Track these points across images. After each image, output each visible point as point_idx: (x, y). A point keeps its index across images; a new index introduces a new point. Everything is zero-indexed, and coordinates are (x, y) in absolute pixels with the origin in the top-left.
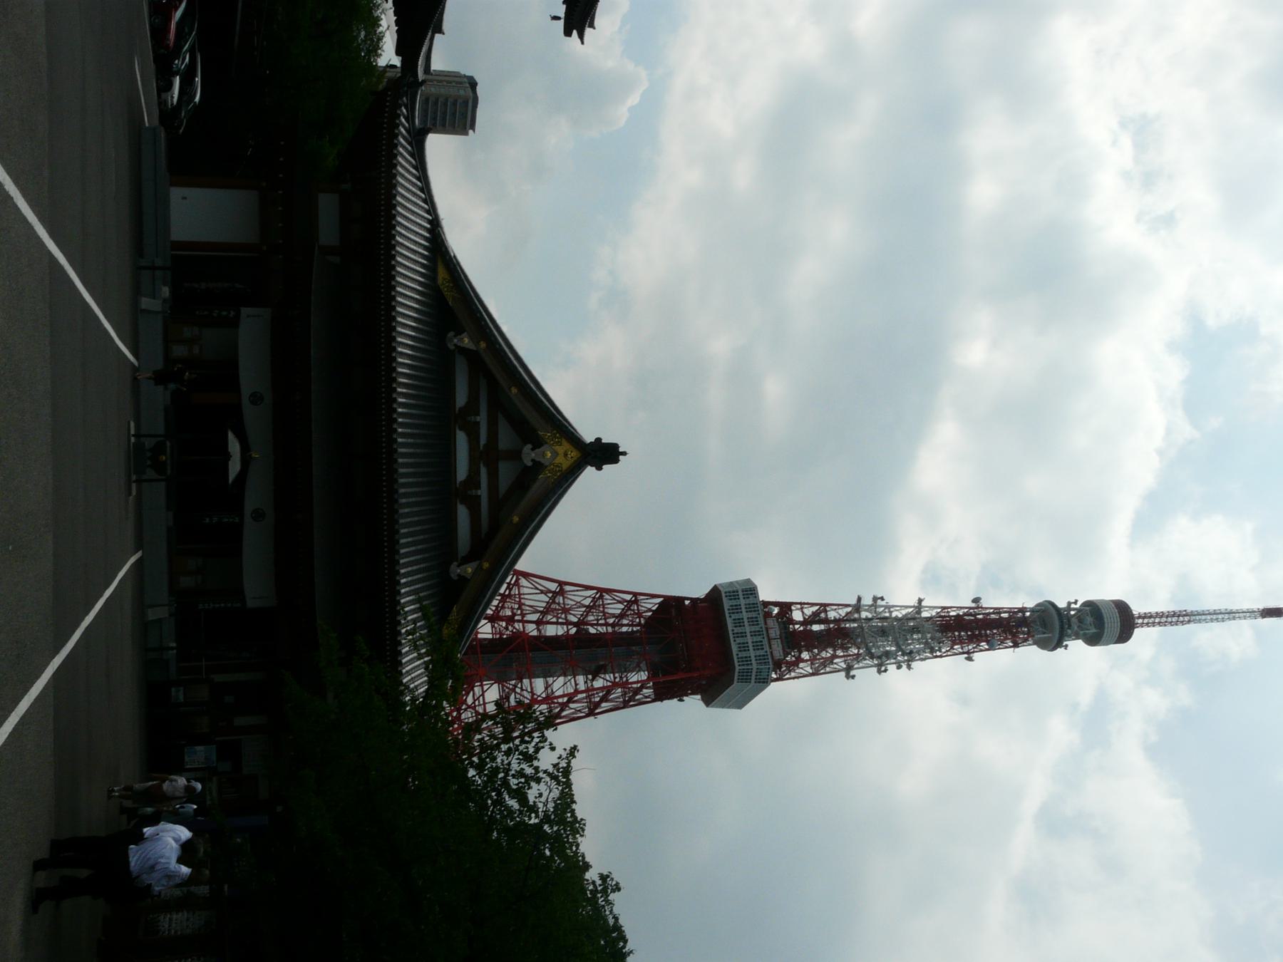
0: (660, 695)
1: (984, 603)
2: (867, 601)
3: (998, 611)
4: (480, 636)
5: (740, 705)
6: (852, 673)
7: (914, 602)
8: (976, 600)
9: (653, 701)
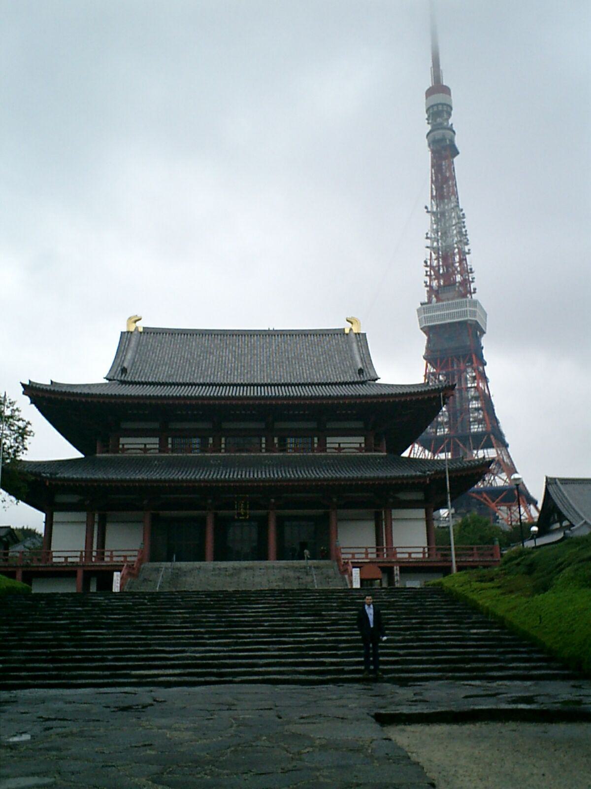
2: (428, 243)
3: (433, 166)
5: (486, 315)
6: (467, 251)
7: (428, 216)
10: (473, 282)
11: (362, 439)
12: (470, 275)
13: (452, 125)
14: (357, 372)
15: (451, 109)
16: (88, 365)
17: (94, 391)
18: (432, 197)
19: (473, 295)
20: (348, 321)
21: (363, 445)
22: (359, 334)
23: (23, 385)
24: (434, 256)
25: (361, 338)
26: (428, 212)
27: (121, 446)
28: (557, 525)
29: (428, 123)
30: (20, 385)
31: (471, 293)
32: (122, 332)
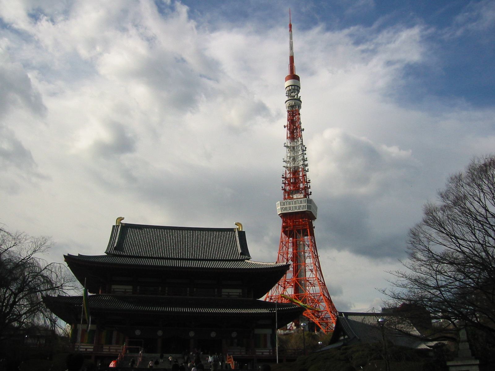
0: (312, 234)
1: (286, 124)
2: (285, 164)
3: (288, 120)
4: (293, 293)
5: (316, 208)
6: (307, 170)
7: (285, 148)
8: (285, 127)
9: (314, 236)
10: (310, 188)
11: (239, 291)
12: (308, 184)
13: (300, 97)
14: (239, 254)
15: (300, 88)
16: (97, 245)
17: (100, 260)
18: (287, 138)
19: (310, 196)
20: (236, 224)
21: (241, 294)
22: (242, 231)
23: (65, 256)
24: (287, 171)
25: (242, 235)
26: (285, 146)
27: (112, 290)
28: (342, 338)
29: (287, 96)
30: (63, 256)
31: (308, 195)
32: (113, 226)
